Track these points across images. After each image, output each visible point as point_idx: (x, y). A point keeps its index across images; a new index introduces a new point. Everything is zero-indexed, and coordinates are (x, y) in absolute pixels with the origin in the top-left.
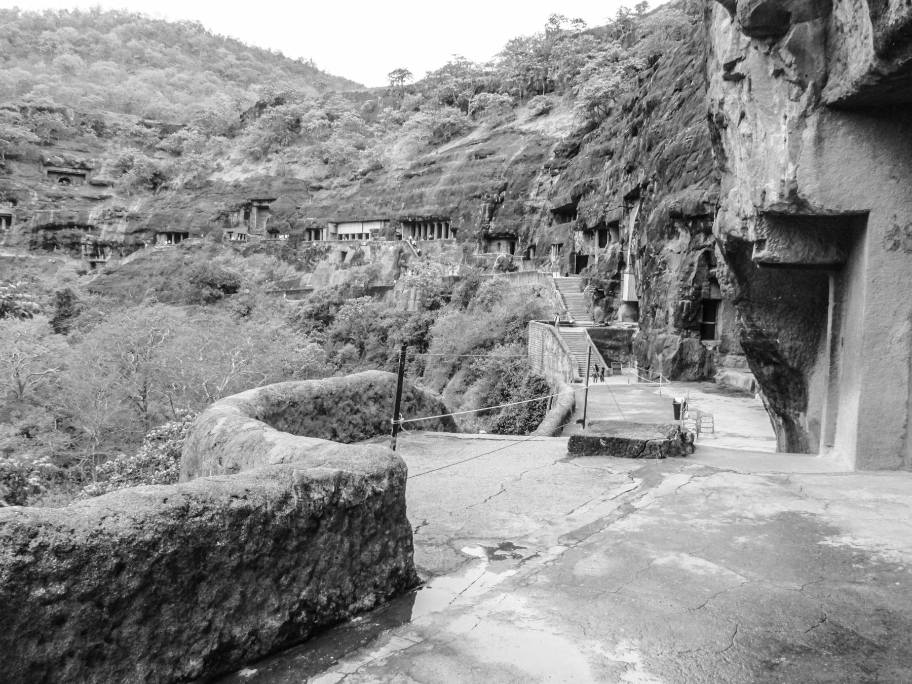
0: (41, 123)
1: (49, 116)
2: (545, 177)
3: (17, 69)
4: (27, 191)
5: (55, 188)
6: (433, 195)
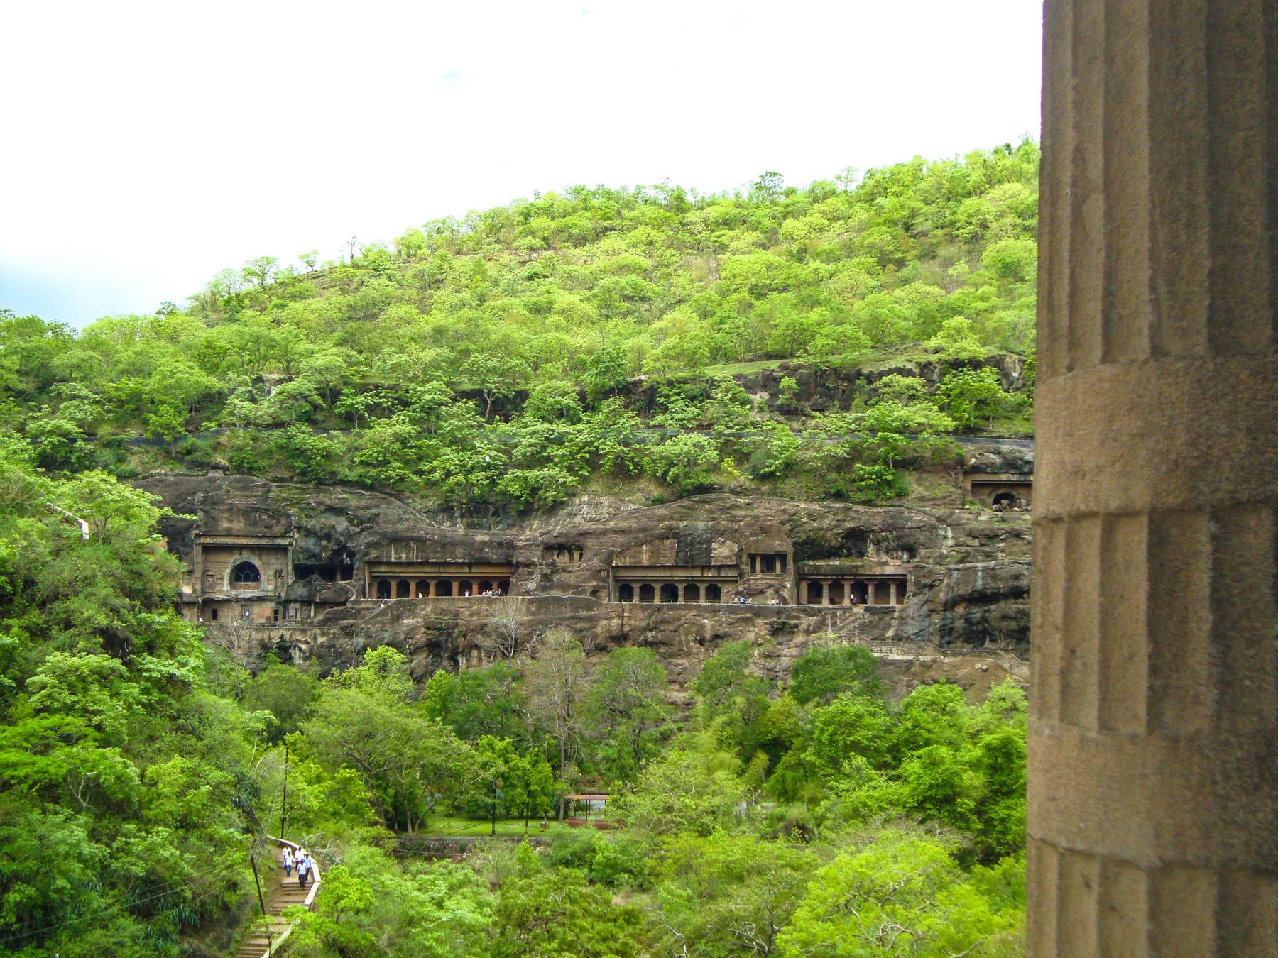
0: (957, 391)
1: (969, 378)
3: (915, 285)
4: (934, 527)
5: (986, 517)
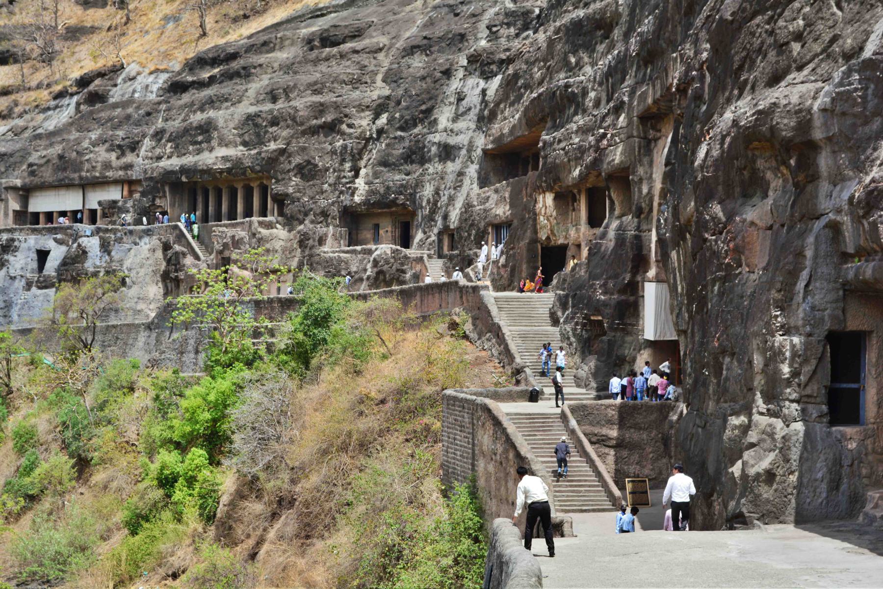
2: (472, 81)
6: (232, 125)
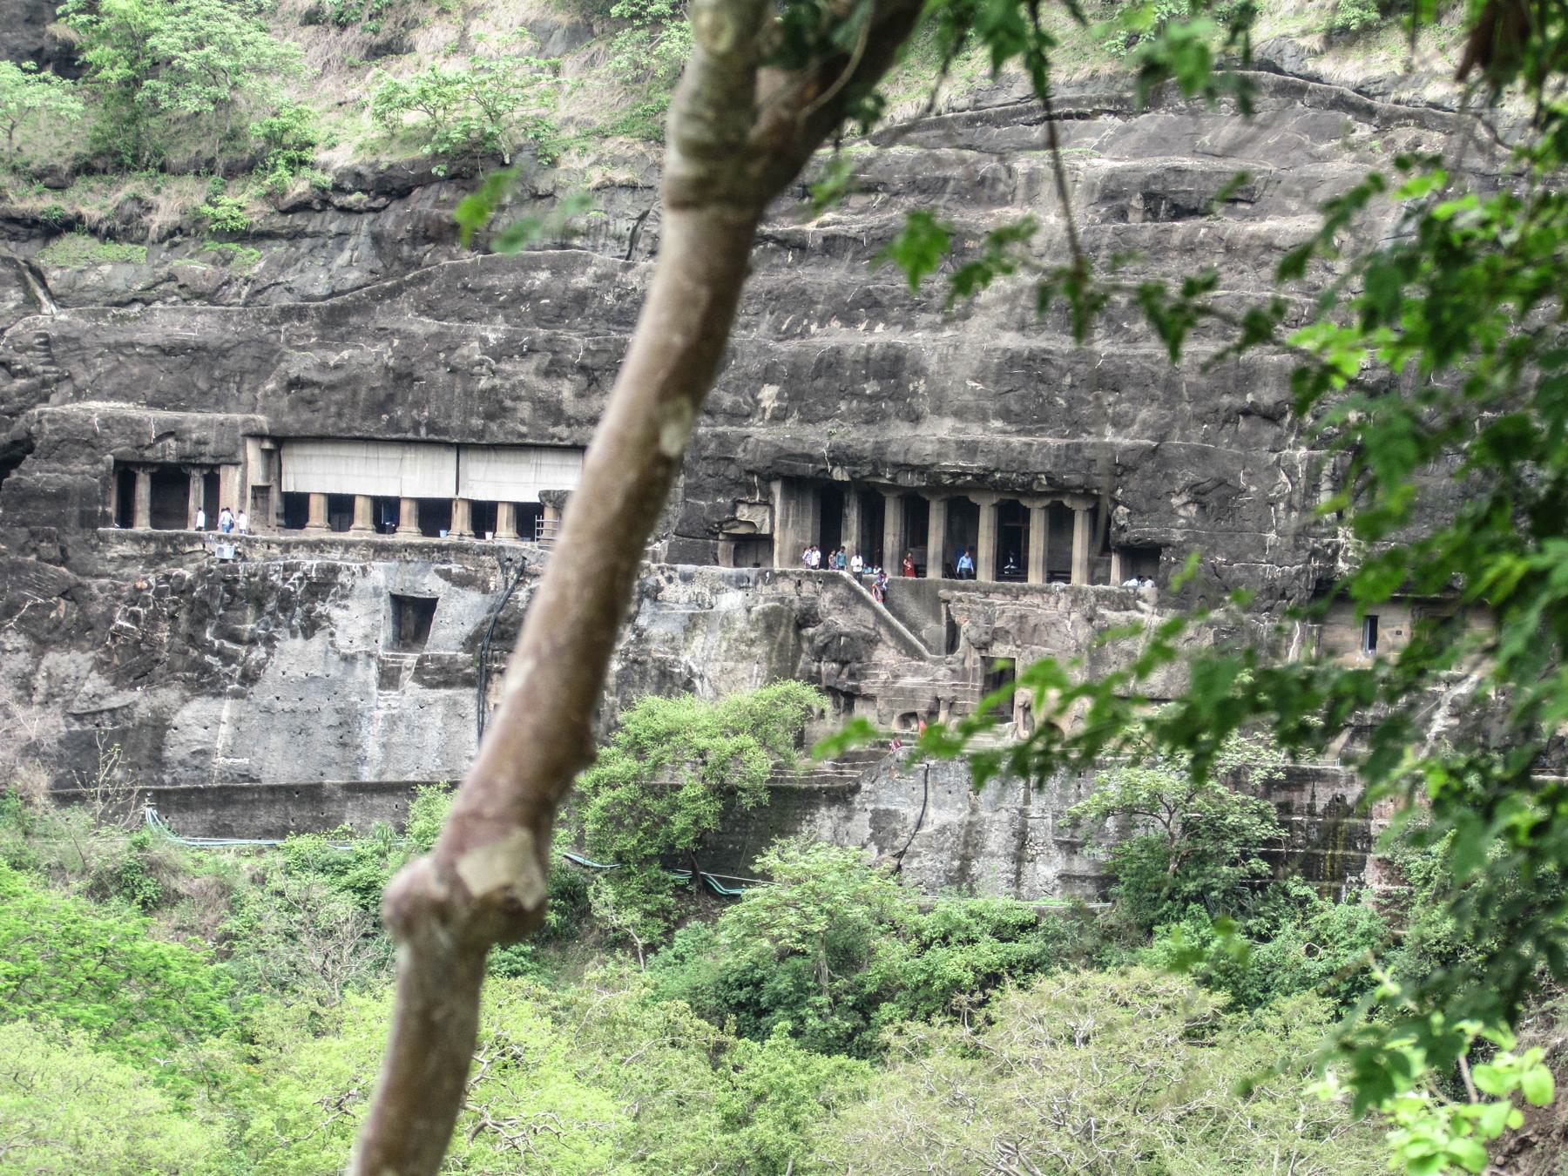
6: (962, 370)
